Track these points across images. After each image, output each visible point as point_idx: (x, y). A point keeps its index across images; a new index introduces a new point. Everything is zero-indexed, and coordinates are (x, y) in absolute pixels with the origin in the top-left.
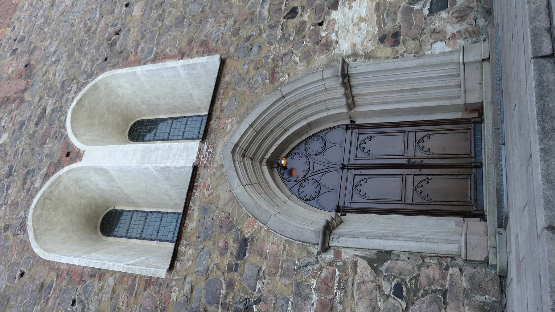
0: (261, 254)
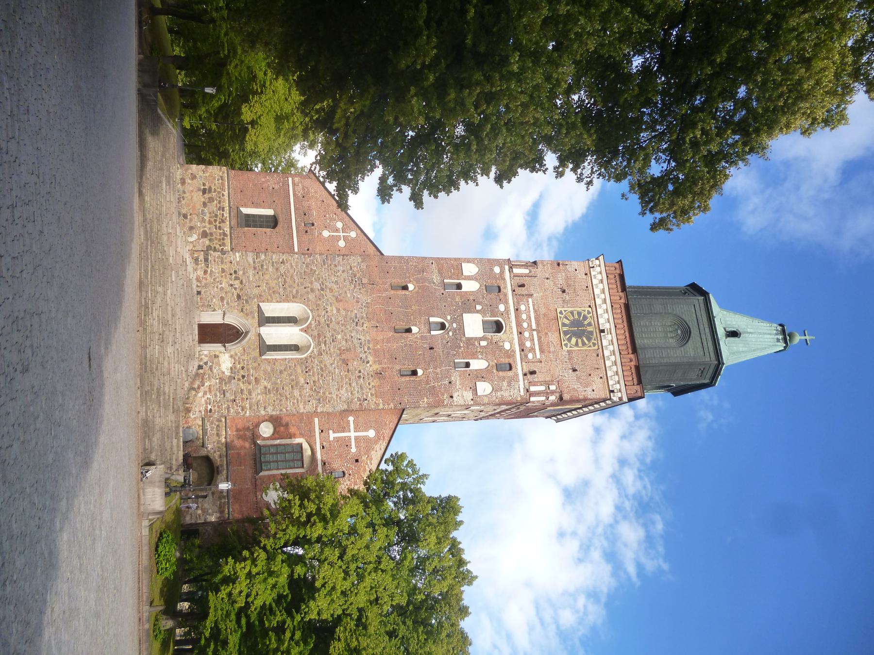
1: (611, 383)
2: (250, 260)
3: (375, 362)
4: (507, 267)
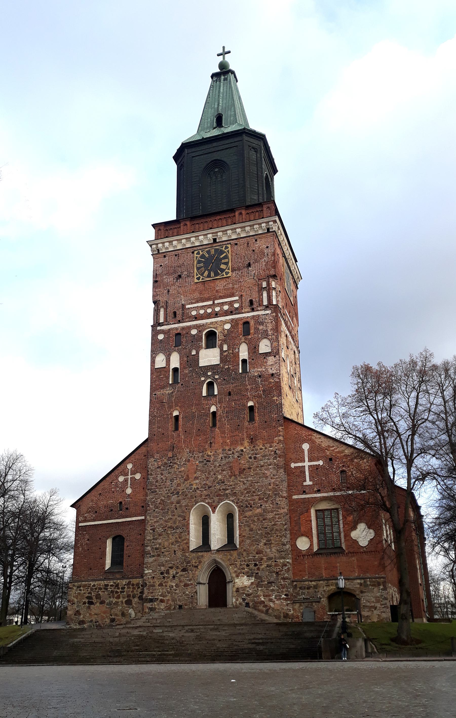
0: (195, 571)
1: (260, 232)
2: (151, 560)
3: (242, 444)
4: (159, 328)
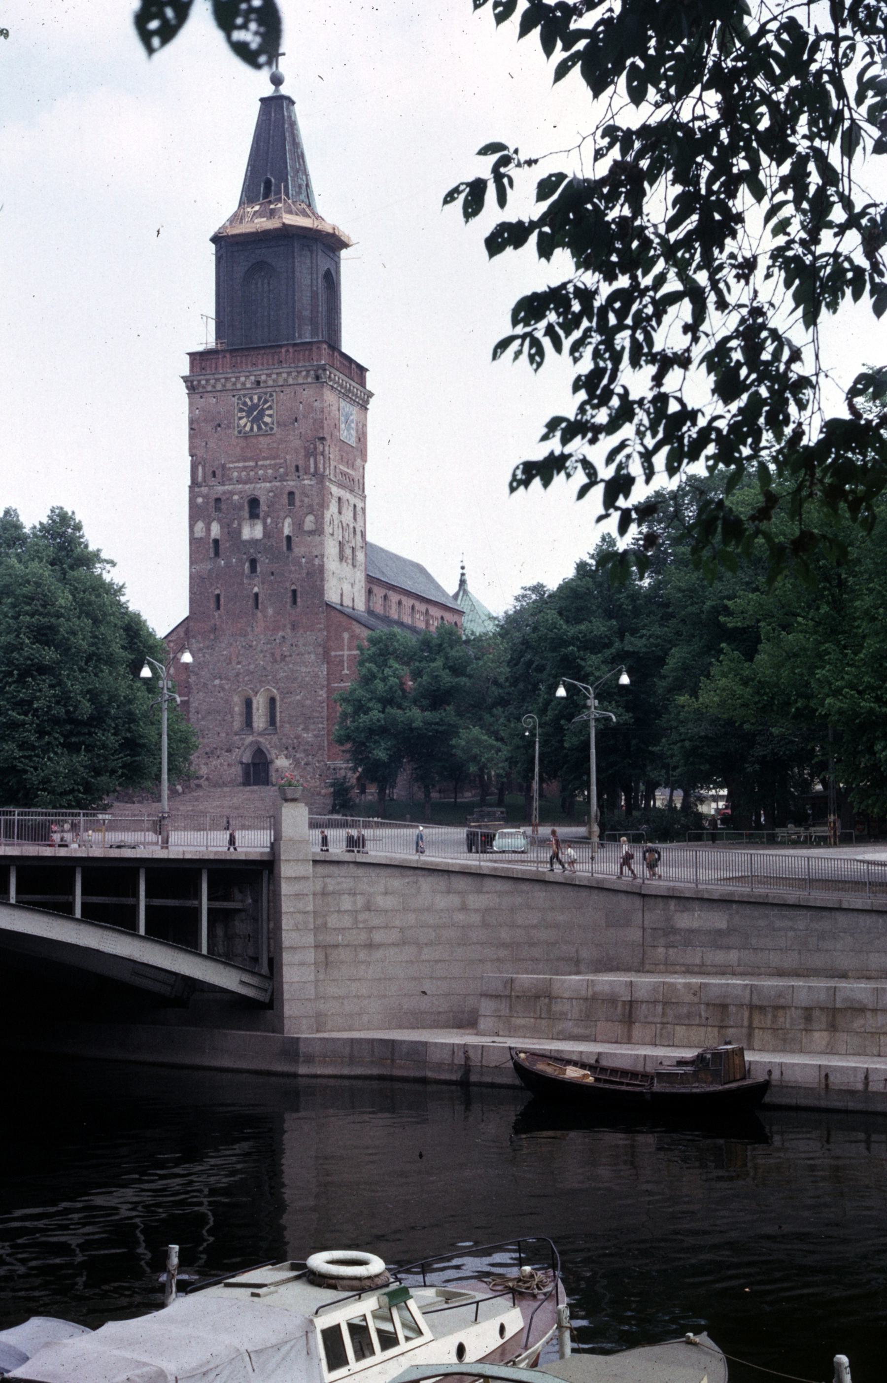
4: (197, 489)
